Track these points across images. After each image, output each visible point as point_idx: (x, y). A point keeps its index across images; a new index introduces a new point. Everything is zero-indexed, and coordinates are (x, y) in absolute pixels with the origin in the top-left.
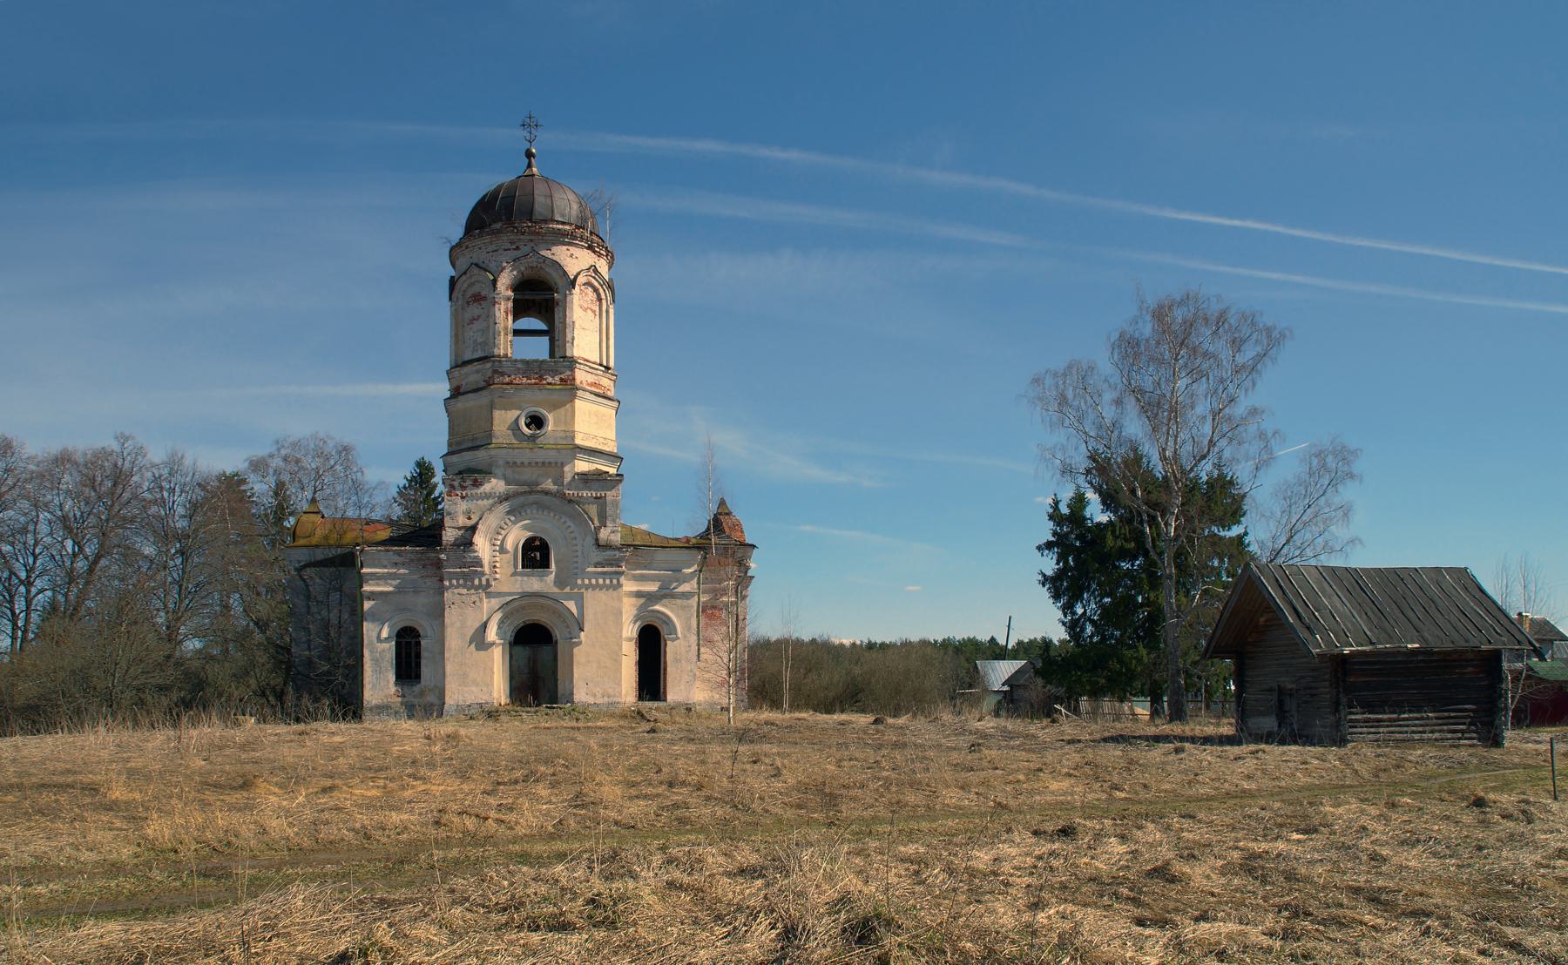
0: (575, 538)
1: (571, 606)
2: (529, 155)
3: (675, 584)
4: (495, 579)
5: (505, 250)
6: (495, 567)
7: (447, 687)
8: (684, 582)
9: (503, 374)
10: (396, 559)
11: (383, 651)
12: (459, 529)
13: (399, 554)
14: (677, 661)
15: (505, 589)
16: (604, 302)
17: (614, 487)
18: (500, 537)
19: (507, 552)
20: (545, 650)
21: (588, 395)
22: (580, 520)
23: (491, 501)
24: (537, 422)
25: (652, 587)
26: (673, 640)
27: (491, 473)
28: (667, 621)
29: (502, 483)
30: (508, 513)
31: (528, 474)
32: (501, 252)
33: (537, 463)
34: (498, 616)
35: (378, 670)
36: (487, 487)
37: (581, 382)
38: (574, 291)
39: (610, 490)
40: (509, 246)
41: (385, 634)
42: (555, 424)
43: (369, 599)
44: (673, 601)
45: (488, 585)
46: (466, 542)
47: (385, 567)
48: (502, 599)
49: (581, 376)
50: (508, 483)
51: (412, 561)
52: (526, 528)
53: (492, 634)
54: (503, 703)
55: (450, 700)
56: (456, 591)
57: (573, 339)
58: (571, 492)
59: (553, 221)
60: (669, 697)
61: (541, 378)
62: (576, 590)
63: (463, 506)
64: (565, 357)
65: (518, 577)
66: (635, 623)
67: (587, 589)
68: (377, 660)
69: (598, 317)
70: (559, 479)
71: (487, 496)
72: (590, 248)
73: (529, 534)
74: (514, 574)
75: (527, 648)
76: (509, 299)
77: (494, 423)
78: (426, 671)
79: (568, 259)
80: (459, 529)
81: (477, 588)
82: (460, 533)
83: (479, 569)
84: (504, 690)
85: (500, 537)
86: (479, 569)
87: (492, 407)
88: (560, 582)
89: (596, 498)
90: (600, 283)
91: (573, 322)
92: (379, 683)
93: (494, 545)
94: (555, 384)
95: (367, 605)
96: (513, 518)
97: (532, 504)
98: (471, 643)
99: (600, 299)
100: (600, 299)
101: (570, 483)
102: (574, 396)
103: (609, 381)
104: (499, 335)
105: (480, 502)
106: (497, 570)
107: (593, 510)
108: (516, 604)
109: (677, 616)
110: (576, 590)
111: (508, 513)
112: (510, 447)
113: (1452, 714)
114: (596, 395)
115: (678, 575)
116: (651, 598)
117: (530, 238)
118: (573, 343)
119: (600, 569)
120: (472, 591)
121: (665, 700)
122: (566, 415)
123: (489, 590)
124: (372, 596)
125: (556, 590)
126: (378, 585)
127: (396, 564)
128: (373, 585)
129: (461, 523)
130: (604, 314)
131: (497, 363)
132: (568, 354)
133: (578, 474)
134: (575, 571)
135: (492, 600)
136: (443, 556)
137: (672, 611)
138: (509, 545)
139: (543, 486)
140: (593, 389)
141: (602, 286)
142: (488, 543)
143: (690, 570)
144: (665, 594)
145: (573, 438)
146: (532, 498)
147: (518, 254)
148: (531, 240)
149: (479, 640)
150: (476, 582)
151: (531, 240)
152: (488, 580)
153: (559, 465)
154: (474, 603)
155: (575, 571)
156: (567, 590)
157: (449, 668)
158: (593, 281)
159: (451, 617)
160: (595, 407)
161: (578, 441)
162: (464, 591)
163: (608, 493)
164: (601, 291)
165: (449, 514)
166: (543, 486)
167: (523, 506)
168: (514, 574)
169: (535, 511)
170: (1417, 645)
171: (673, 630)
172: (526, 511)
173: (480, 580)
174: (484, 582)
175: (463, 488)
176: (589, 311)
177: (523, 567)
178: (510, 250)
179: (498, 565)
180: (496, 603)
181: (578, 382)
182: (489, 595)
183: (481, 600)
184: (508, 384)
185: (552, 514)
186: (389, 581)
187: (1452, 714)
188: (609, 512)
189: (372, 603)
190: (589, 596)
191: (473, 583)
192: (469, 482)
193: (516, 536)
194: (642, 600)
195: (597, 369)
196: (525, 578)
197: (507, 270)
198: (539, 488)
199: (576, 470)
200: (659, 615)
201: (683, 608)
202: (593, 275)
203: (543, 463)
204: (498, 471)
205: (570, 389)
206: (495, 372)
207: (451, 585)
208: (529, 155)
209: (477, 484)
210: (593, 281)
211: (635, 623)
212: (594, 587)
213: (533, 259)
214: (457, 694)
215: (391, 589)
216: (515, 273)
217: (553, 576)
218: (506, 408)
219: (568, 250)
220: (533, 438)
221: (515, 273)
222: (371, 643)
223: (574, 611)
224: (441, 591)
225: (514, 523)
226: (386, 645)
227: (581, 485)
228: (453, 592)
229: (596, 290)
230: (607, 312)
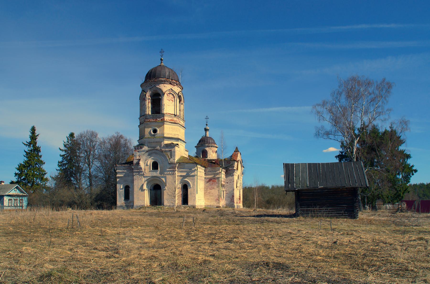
0: (164, 161)
1: (164, 179)
2: (161, 60)
3: (190, 173)
4: (145, 173)
5: (149, 86)
6: (145, 169)
7: (134, 201)
8: (193, 172)
9: (147, 119)
10: (124, 168)
11: (121, 192)
12: (137, 160)
13: (124, 166)
14: (191, 194)
15: (148, 175)
16: (176, 98)
17: (174, 147)
18: (146, 162)
19: (148, 166)
20: (159, 191)
21: (168, 123)
22: (164, 156)
23: (145, 152)
24: (155, 131)
25: (184, 174)
26: (190, 188)
27: (144, 145)
28: (188, 183)
29: (147, 147)
30: (148, 155)
31: (153, 145)
32: (148, 87)
33: (155, 142)
34: (146, 182)
35: (120, 197)
36: (143, 149)
37: (167, 120)
38: (164, 96)
39: (173, 148)
40: (149, 85)
41: (122, 187)
42: (160, 131)
43: (118, 178)
44: (190, 178)
45: (144, 174)
46: (138, 164)
47: (122, 170)
48: (147, 178)
49: (166, 118)
50: (148, 147)
51: (127, 168)
52: (152, 159)
53: (145, 187)
54: (148, 205)
55: (135, 205)
56: (136, 176)
57: (164, 108)
58: (163, 149)
59: (160, 78)
60: (189, 204)
61: (156, 119)
62: (164, 175)
63: (138, 154)
64: (162, 113)
65: (151, 172)
66: (180, 184)
67: (167, 175)
68: (120, 194)
69: (174, 102)
70: (160, 146)
71: (144, 151)
72: (170, 84)
73: (153, 161)
74: (150, 171)
75: (154, 191)
76: (149, 99)
77: (145, 132)
78: (130, 197)
79: (164, 88)
80: (137, 160)
81: (141, 175)
82: (137, 161)
83: (141, 170)
84: (149, 202)
85: (146, 162)
86: (141, 170)
87: (145, 127)
88: (161, 173)
89: (170, 150)
90: (174, 93)
91: (164, 104)
92: (120, 200)
93: (145, 164)
94: (160, 121)
95: (118, 180)
96: (149, 157)
97: (154, 153)
98: (140, 189)
99: (174, 97)
100: (174, 97)
101: (163, 147)
102: (164, 124)
103: (177, 119)
104: (147, 109)
105: (142, 153)
106: (146, 170)
107: (169, 154)
108: (150, 179)
109: (191, 182)
110: (164, 175)
111: (148, 155)
112: (149, 138)
113: (338, 208)
114: (171, 123)
115: (191, 170)
116: (184, 177)
117: (154, 83)
118: (164, 110)
119: (170, 170)
120: (140, 176)
121: (188, 204)
122: (162, 129)
123: (144, 176)
124: (119, 177)
125: (160, 175)
126: (120, 175)
127: (124, 169)
128: (119, 175)
129: (138, 158)
130: (176, 101)
131: (146, 116)
132: (163, 113)
133: (165, 144)
134: (164, 170)
135: (145, 178)
136: (133, 167)
137: (190, 180)
138: (149, 164)
139: (157, 148)
140: (171, 121)
142: (143, 163)
143: (194, 169)
144: (188, 176)
145: (164, 135)
146: (153, 151)
147: (151, 87)
148: (154, 83)
149: (142, 189)
150: (141, 174)
151: (154, 83)
152: (143, 173)
153: (160, 142)
154: (141, 179)
155: (164, 170)
156: (162, 175)
157: (135, 196)
158: (172, 92)
159: (135, 183)
160: (172, 126)
161: (165, 135)
162: (138, 176)
163: (172, 149)
164: (174, 95)
165: (135, 156)
166: (157, 148)
167: (152, 153)
168: (150, 171)
169: (154, 155)
170: (323, 187)
171: (190, 186)
172: (152, 155)
173: (142, 173)
174: (143, 174)
175: (138, 149)
176: (171, 101)
177: (152, 170)
178: (149, 86)
179: (146, 169)
180: (146, 179)
181: (165, 120)
182: (144, 177)
183: (142, 178)
184: (149, 121)
185: (158, 155)
186: (123, 174)
187: (338, 208)
188: (173, 154)
189: (119, 179)
190: (168, 176)
191: (140, 174)
192: (139, 148)
193: (150, 162)
194: (182, 178)
195: (172, 116)
196: (152, 172)
197: (149, 92)
198: (156, 149)
199: (165, 143)
200: (186, 181)
201: (192, 179)
202: (171, 91)
203: (157, 142)
204: (146, 144)
205: (163, 121)
206: (146, 118)
207: (135, 174)
208: (161, 60)
209: (141, 148)
210: (172, 92)
211: (180, 184)
212: (169, 174)
213: (155, 88)
214: (137, 203)
215: (123, 176)
216: (151, 92)
217: (159, 172)
218: (148, 128)
219: (164, 85)
220: (154, 135)
221: (151, 92)
222: (118, 189)
223: (164, 181)
224: (133, 176)
225: (150, 158)
226: (122, 190)
227: (166, 147)
228: (136, 176)
229: (173, 95)
230: (176, 100)
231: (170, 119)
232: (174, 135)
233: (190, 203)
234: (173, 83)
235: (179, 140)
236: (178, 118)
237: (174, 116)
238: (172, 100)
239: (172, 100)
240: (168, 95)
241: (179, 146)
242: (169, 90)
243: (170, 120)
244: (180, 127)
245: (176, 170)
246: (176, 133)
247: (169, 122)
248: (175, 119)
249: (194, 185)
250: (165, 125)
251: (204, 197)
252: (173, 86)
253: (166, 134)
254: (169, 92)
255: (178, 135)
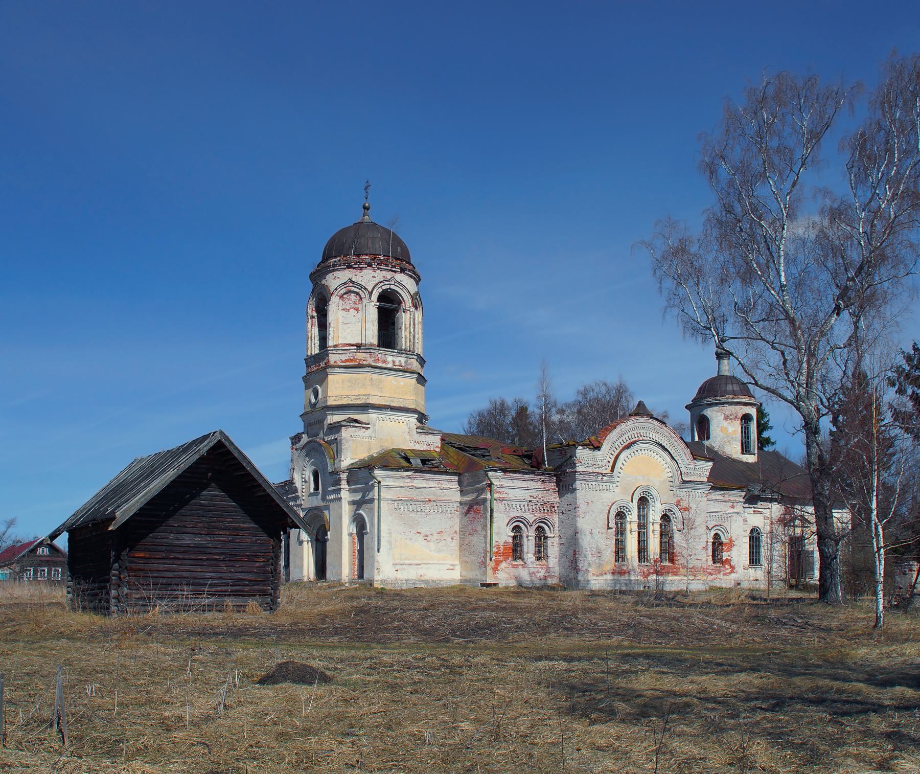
21: (337, 370)
37: (335, 362)
72: (349, 267)
90: (359, 289)
103: (365, 355)
109: (368, 517)
114: (345, 368)
121: (363, 578)
140: (348, 364)
141: (360, 289)
158: (353, 289)
160: (348, 376)
161: (331, 402)
164: (361, 293)
176: (352, 311)
181: (332, 363)
195: (350, 349)
202: (351, 285)
229: (358, 294)
231: (344, 357)
232: (355, 397)
233: (366, 575)
234: (356, 264)
235: (367, 408)
236: (368, 351)
237: (355, 348)
238: (356, 306)
239: (355, 309)
240: (344, 296)
241: (367, 426)
242: (345, 283)
243: (346, 361)
244: (375, 373)
245: (340, 490)
246: (362, 392)
247: (340, 367)
248: (360, 355)
249: (372, 525)
250: (329, 376)
251: (460, 558)
252: (357, 272)
253: (332, 399)
254: (344, 291)
255: (366, 397)
